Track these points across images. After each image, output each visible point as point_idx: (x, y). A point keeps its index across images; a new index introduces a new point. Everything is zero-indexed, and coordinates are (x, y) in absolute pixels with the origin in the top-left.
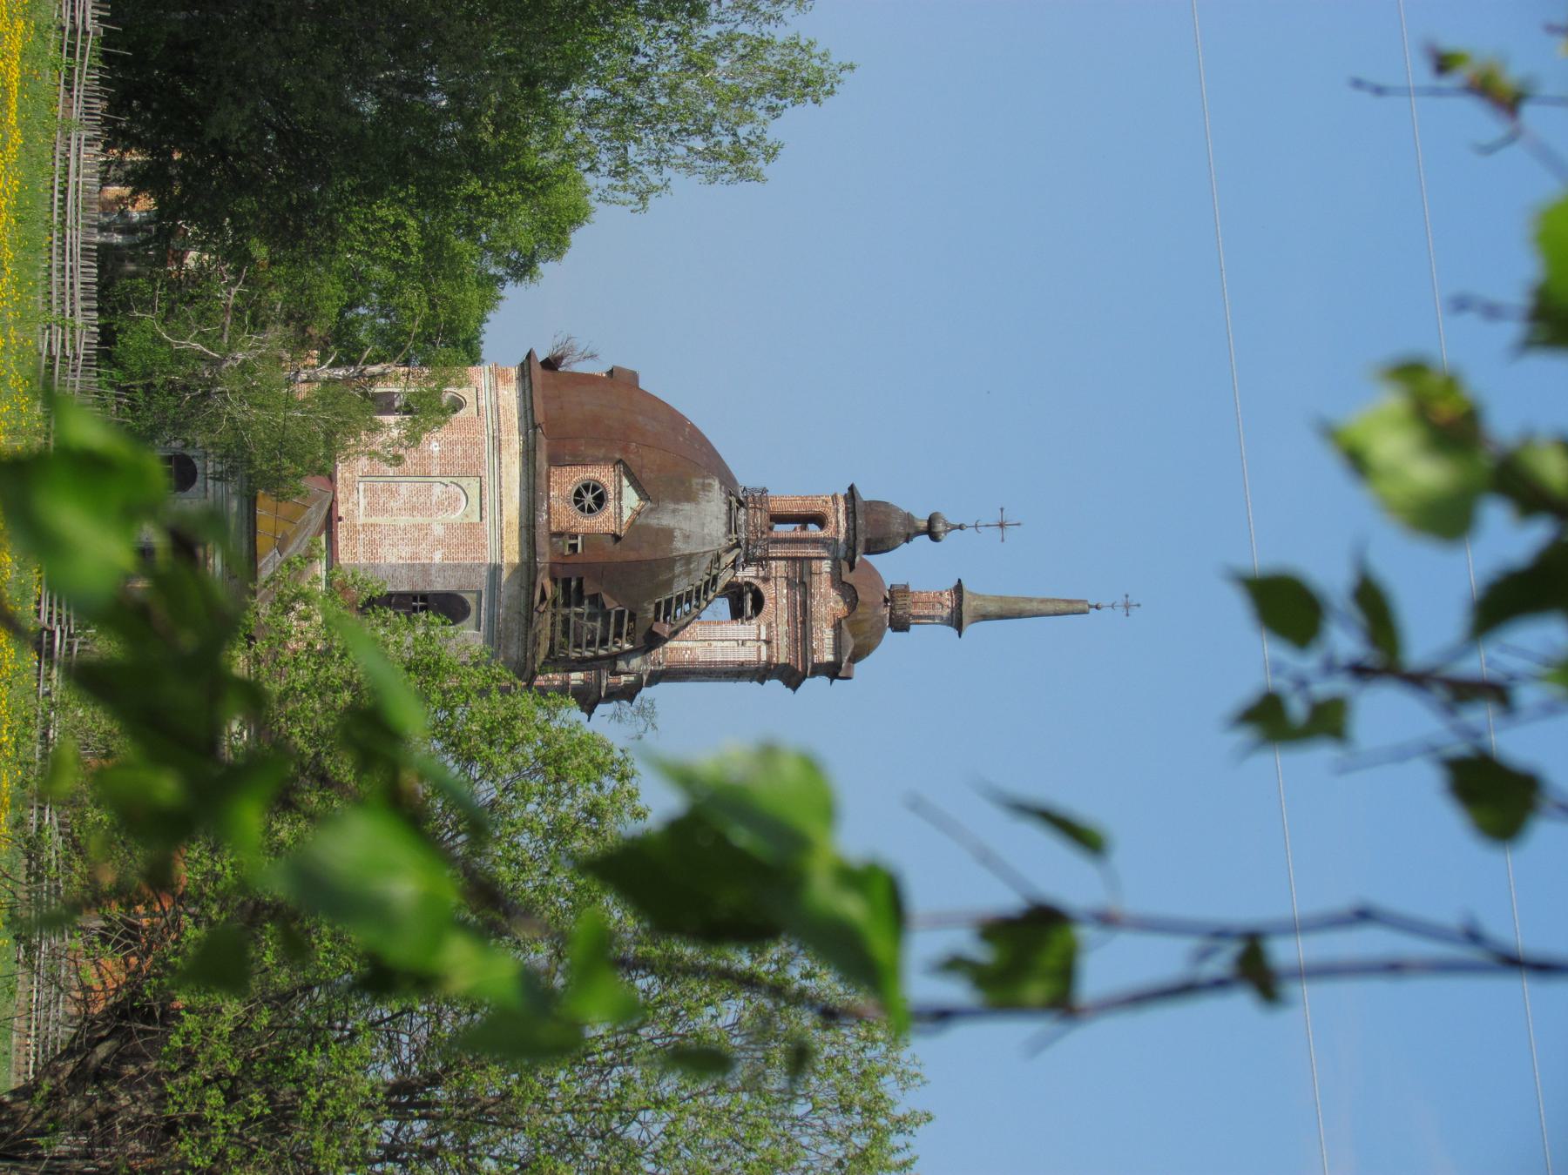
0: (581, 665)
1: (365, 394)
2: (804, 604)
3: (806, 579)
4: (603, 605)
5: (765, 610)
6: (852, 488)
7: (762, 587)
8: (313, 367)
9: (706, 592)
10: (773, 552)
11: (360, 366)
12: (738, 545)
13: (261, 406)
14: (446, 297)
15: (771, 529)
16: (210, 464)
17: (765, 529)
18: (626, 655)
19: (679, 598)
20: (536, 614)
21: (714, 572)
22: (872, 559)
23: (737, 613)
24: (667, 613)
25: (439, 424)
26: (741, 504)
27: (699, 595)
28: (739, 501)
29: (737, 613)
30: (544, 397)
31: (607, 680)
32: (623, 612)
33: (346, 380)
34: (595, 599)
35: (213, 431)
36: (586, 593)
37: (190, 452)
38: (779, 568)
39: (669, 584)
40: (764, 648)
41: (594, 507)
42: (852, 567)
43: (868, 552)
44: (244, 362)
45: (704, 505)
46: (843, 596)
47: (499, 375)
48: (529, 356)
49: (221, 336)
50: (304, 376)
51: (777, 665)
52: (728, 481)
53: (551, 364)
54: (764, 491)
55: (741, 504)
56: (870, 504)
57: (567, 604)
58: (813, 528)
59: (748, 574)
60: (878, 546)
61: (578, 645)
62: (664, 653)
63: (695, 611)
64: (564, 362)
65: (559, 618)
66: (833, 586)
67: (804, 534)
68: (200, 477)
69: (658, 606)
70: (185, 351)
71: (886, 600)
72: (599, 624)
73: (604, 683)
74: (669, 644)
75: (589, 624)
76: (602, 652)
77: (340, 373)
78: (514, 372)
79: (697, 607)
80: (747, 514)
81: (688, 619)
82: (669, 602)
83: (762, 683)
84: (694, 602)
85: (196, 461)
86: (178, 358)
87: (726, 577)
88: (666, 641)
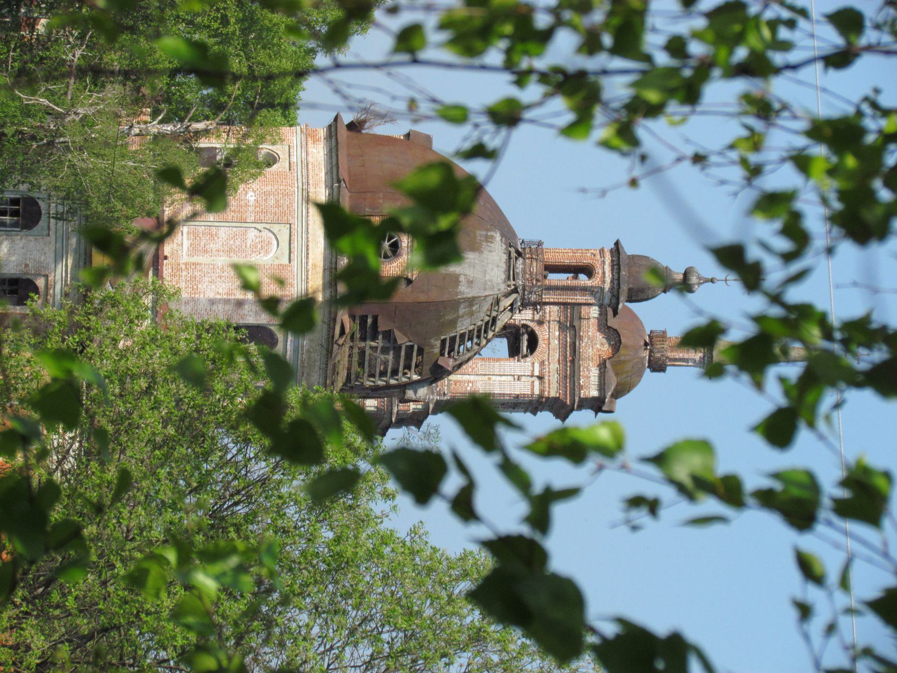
0: (374, 392)
1: (191, 149)
2: (573, 345)
3: (576, 323)
4: (395, 340)
5: (539, 349)
6: (617, 244)
7: (536, 329)
8: (146, 123)
9: (486, 332)
10: (547, 298)
11: (186, 123)
12: (515, 291)
13: (97, 156)
14: (263, 64)
15: (545, 277)
16: (53, 205)
17: (540, 277)
18: (414, 385)
19: (462, 336)
20: (335, 346)
21: (494, 314)
22: (633, 306)
23: (514, 351)
24: (451, 350)
25: (254, 176)
26: (519, 254)
27: (480, 334)
28: (518, 252)
29: (514, 351)
30: (349, 155)
31: (398, 408)
32: (412, 347)
33: (174, 136)
34: (388, 335)
35: (56, 176)
36: (380, 329)
37: (35, 194)
38: (552, 312)
39: (453, 323)
40: (537, 383)
41: (389, 253)
42: (615, 313)
43: (630, 300)
44: (85, 116)
45: (486, 254)
46: (608, 339)
47: (309, 134)
48: (336, 119)
49: (66, 93)
50: (137, 131)
51: (548, 398)
52: (509, 235)
53: (354, 127)
54: (540, 244)
55: (519, 254)
56: (633, 257)
57: (363, 339)
58: (582, 277)
59: (525, 317)
60: (639, 295)
61: (372, 375)
62: (449, 385)
63: (476, 347)
64: (367, 125)
65: (356, 351)
66: (599, 330)
67: (575, 283)
68: (44, 218)
69: (444, 341)
70: (33, 105)
71: (646, 344)
72: (391, 357)
73: (395, 410)
74: (453, 377)
75: (382, 356)
76: (393, 382)
77: (168, 128)
78: (322, 133)
79: (478, 344)
80: (524, 264)
81: (469, 355)
82: (453, 339)
83: (535, 413)
84: (475, 340)
85: (41, 203)
86: (27, 111)
87: (504, 319)
88: (450, 373)
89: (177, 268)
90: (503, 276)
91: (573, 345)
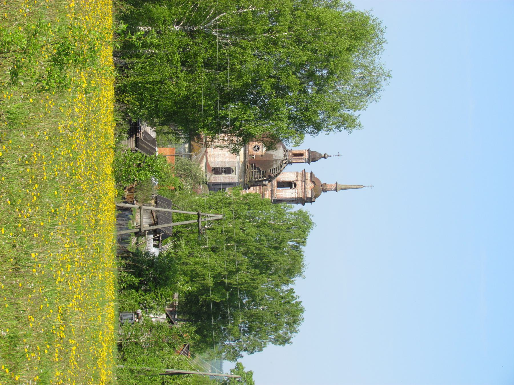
12: (286, 159)
26: (287, 151)
39: (272, 165)
45: (279, 150)
55: (287, 151)
69: (270, 170)
89: (210, 155)
91: (305, 185)
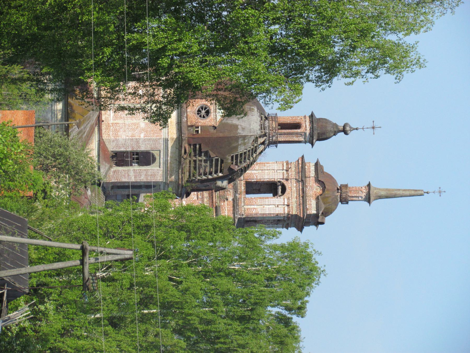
4: (210, 156)
9: (252, 154)
12: (265, 135)
28: (265, 117)
36: (202, 150)
39: (236, 148)
65: (192, 161)
69: (232, 157)
82: (237, 156)
89: (108, 126)
90: (259, 127)
